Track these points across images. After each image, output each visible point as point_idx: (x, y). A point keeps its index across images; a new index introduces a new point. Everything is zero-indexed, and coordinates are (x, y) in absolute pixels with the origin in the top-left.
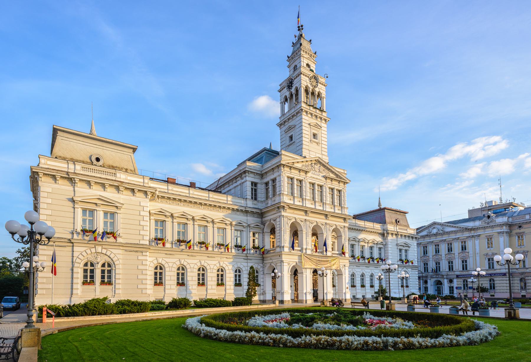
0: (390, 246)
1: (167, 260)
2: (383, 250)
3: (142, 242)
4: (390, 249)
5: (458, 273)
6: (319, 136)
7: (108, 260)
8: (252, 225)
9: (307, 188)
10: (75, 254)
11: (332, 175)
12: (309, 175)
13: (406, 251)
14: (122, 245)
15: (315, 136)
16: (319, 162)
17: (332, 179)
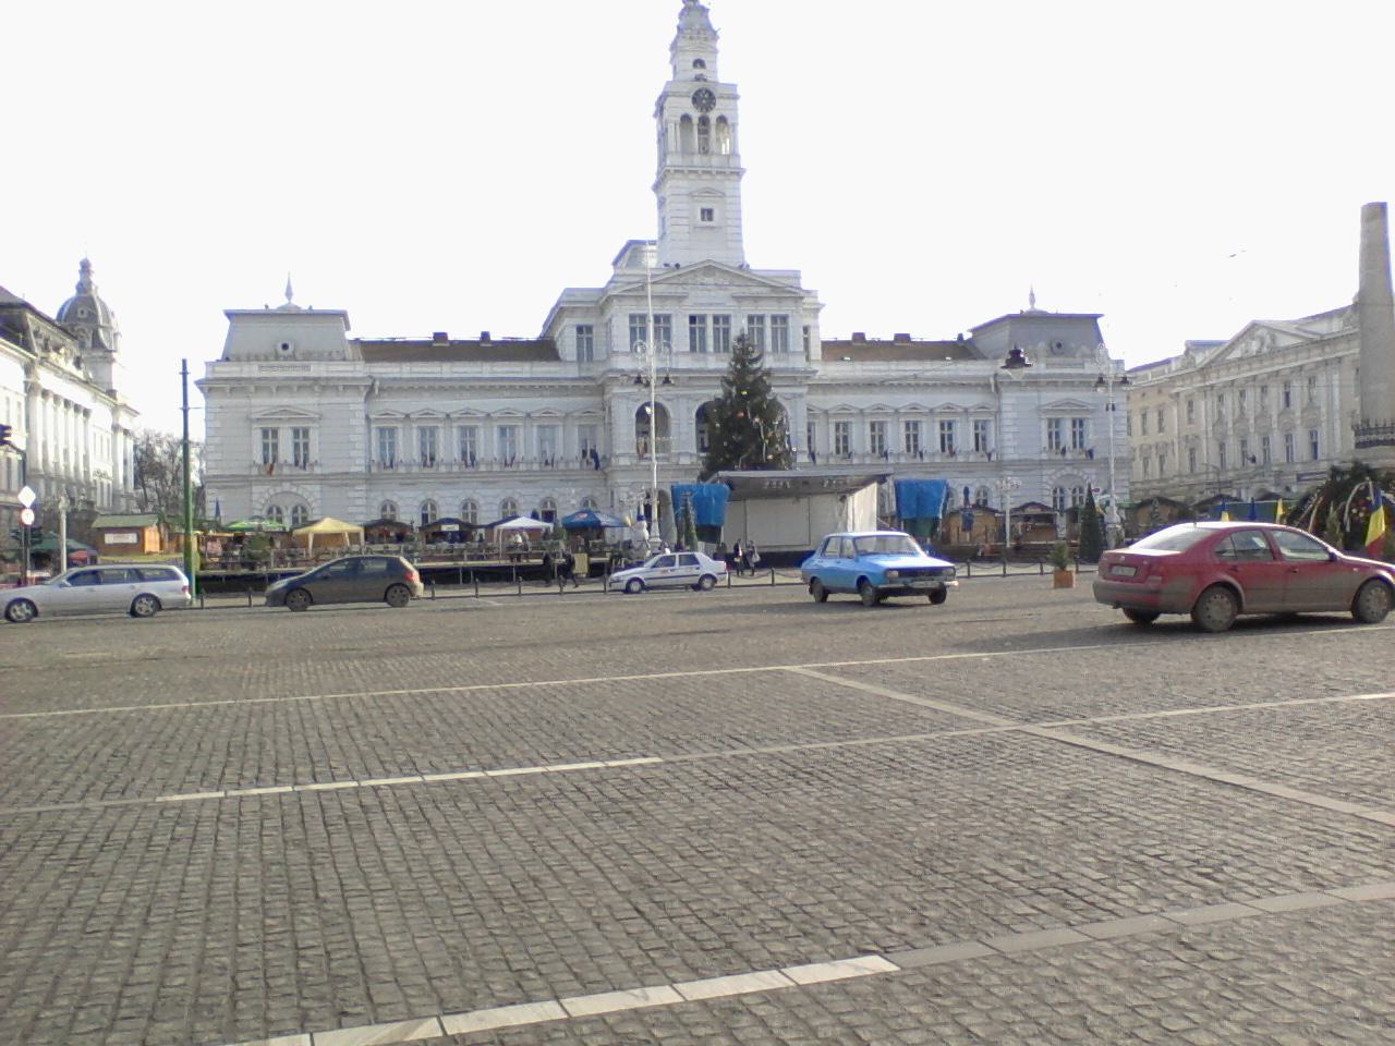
0: (1004, 415)
1: (523, 492)
2: (992, 427)
3: (354, 469)
4: (1008, 422)
5: (1299, 468)
6: (716, 215)
7: (297, 501)
8: (576, 414)
9: (680, 328)
10: (255, 497)
11: (756, 290)
12: (688, 302)
13: (1079, 423)
14: (323, 478)
15: (708, 214)
16: (710, 269)
17: (756, 299)
